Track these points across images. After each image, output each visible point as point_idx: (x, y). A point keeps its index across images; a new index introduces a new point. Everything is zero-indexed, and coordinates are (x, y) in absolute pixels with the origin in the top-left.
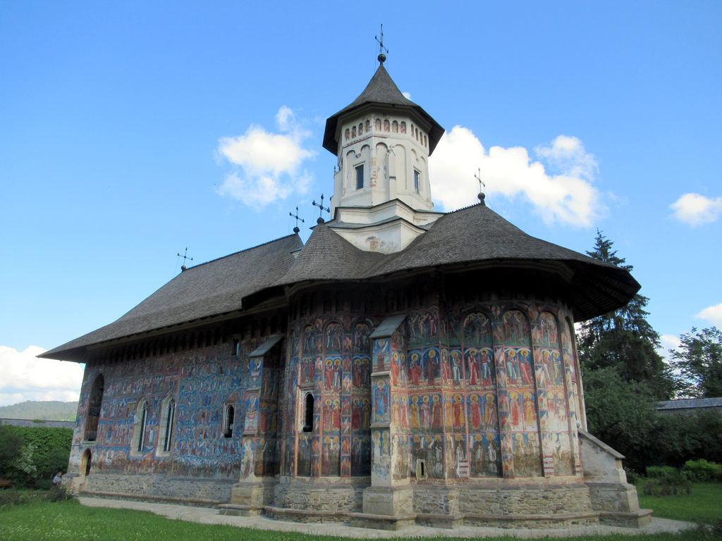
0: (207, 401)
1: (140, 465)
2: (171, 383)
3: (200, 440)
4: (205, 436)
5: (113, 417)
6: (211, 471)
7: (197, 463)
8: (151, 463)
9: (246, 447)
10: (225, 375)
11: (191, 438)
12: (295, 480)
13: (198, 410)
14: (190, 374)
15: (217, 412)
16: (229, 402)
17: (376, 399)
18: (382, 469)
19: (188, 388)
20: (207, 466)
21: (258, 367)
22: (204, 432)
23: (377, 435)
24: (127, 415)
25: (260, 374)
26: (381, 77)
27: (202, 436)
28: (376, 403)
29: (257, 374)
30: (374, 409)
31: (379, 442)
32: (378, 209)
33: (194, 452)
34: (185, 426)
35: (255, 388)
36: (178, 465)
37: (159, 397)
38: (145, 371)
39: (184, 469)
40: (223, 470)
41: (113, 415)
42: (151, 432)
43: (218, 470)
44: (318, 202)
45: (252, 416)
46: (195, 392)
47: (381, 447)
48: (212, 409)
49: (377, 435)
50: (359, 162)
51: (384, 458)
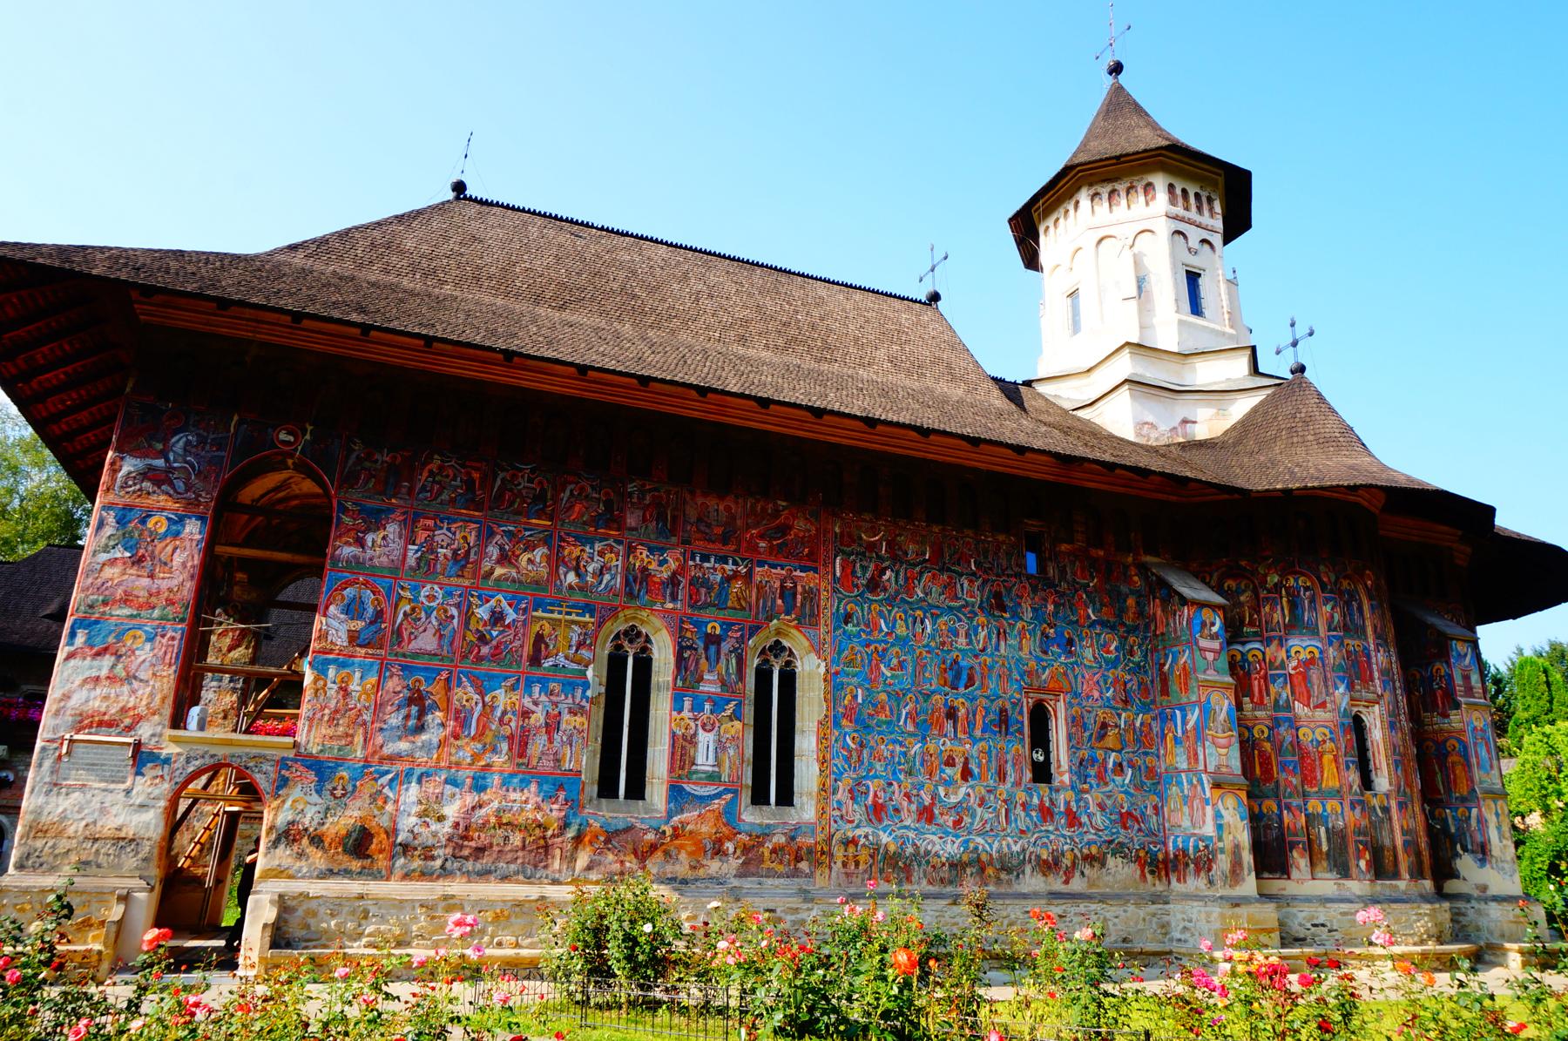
0: (955, 675)
1: (653, 848)
2: (787, 593)
3: (948, 783)
4: (966, 774)
5: (417, 654)
6: (1009, 871)
7: (949, 848)
8: (720, 841)
9: (1223, 812)
10: (1016, 616)
11: (909, 773)
12: (1378, 888)
13: (927, 696)
14: (874, 585)
15: (1003, 711)
16: (1039, 689)
17: (1475, 744)
18: (1506, 866)
19: (872, 626)
20: (984, 858)
21: (1215, 629)
22: (959, 761)
23: (1490, 809)
24: (535, 660)
25: (1222, 648)
26: (1120, 104)
27: (954, 772)
28: (1476, 752)
29: (1216, 645)
30: (1474, 760)
31: (1494, 818)
32: (1165, 357)
33: (926, 814)
34: (873, 739)
35: (1211, 676)
36: (864, 856)
37: (727, 626)
38: (631, 521)
39: (895, 866)
40: (1048, 866)
41: (426, 641)
42: (705, 739)
43: (1028, 869)
44: (1301, 330)
45: (1223, 742)
46: (902, 641)
47: (1499, 828)
48: (985, 702)
49: (1490, 809)
50: (1195, 264)
51: (1505, 846)
